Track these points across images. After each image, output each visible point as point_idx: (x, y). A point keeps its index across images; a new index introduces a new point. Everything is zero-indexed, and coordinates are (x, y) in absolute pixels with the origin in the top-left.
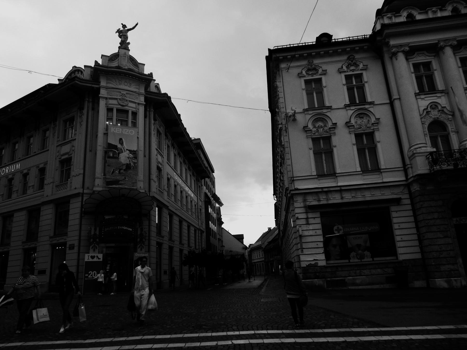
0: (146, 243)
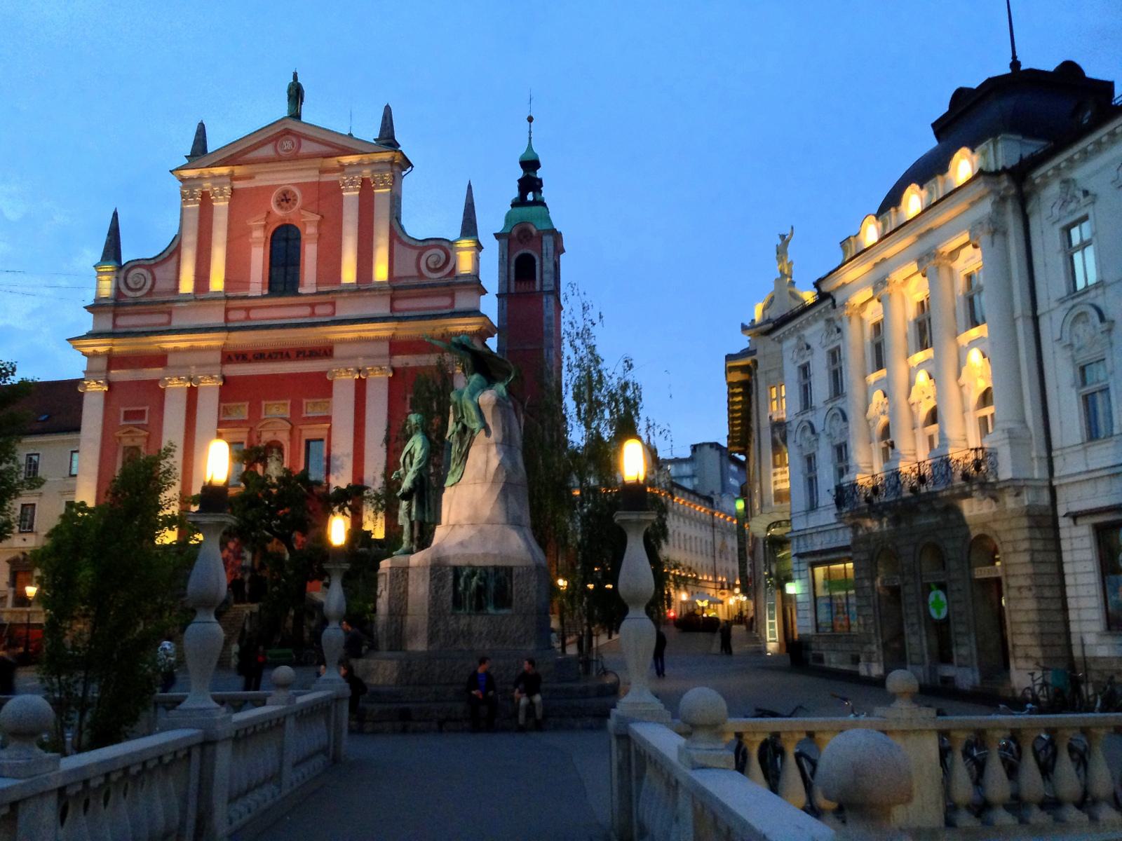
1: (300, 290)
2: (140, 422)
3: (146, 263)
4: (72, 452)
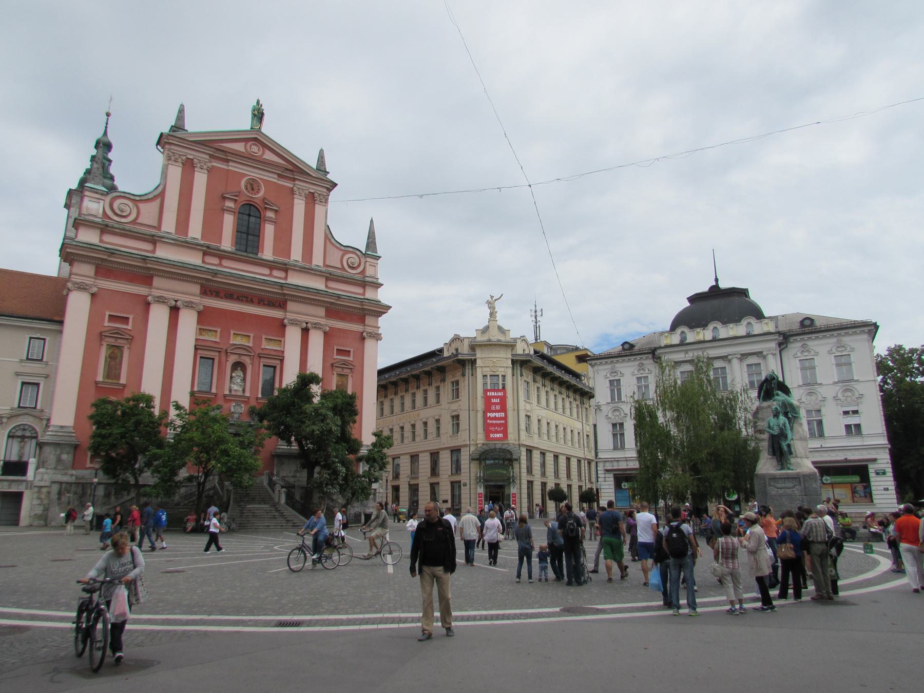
0: (518, 482)
1: (260, 255)
2: (125, 327)
3: (132, 197)
4: (31, 338)
